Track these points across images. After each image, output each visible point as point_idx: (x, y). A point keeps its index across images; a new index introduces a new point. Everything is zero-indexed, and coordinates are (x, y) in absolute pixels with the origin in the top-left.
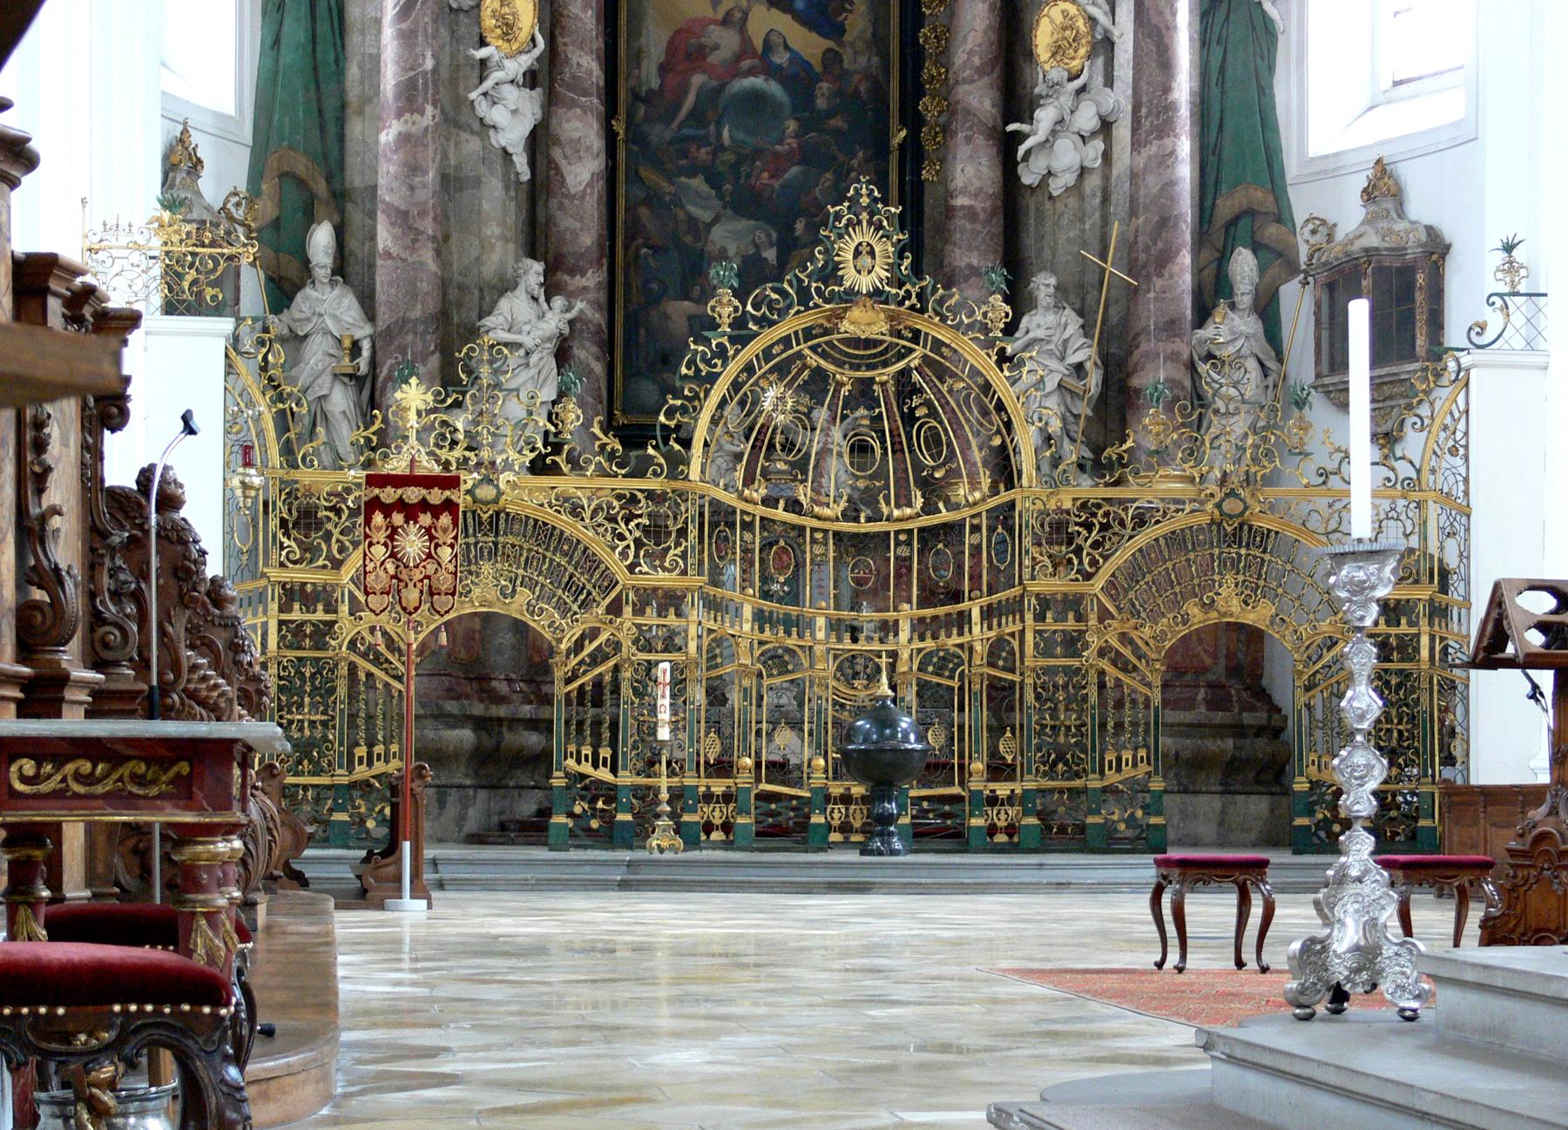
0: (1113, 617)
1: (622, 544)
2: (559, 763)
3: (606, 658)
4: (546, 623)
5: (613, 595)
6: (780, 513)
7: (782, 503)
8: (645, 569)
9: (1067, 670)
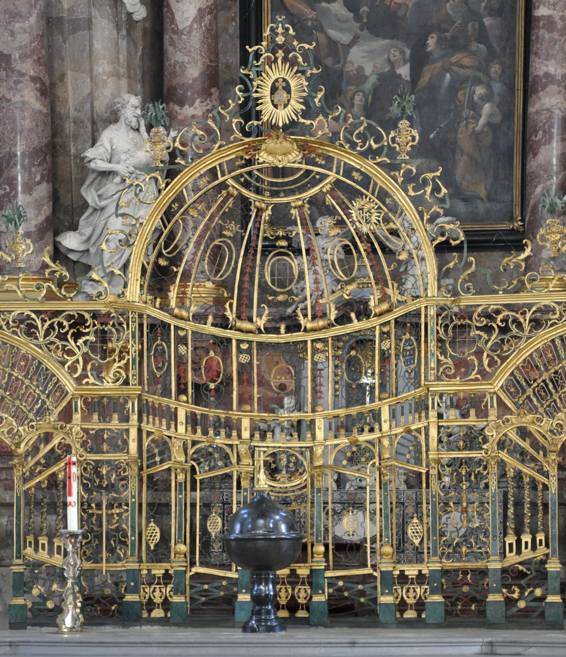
0: (512, 413)
1: (71, 360)
2: (19, 551)
3: (58, 459)
4: (6, 430)
5: (64, 404)
6: (209, 329)
7: (210, 319)
8: (92, 380)
9: (468, 462)
